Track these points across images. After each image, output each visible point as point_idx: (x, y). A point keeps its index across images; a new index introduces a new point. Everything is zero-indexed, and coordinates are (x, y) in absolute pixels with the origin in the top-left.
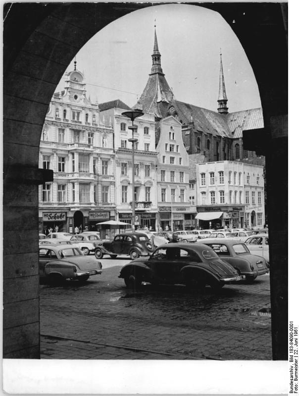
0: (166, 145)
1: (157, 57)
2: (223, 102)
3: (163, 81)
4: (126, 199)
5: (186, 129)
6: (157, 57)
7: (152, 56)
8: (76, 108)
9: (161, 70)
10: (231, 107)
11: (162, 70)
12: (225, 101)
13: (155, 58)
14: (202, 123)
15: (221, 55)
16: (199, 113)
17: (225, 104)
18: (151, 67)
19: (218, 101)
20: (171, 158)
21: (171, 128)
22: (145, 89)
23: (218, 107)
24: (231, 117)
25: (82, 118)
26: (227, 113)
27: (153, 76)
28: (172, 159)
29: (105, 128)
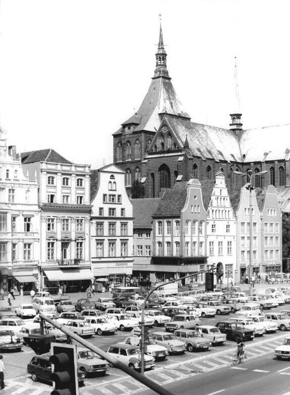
0: (105, 195)
1: (162, 57)
3: (169, 87)
5: (179, 154)
6: (162, 57)
7: (156, 55)
9: (167, 73)
11: (167, 73)
13: (160, 58)
14: (202, 145)
16: (201, 132)
17: (239, 118)
19: (231, 115)
20: (110, 209)
21: (112, 177)
24: (244, 136)
28: (112, 210)
29: (28, 183)
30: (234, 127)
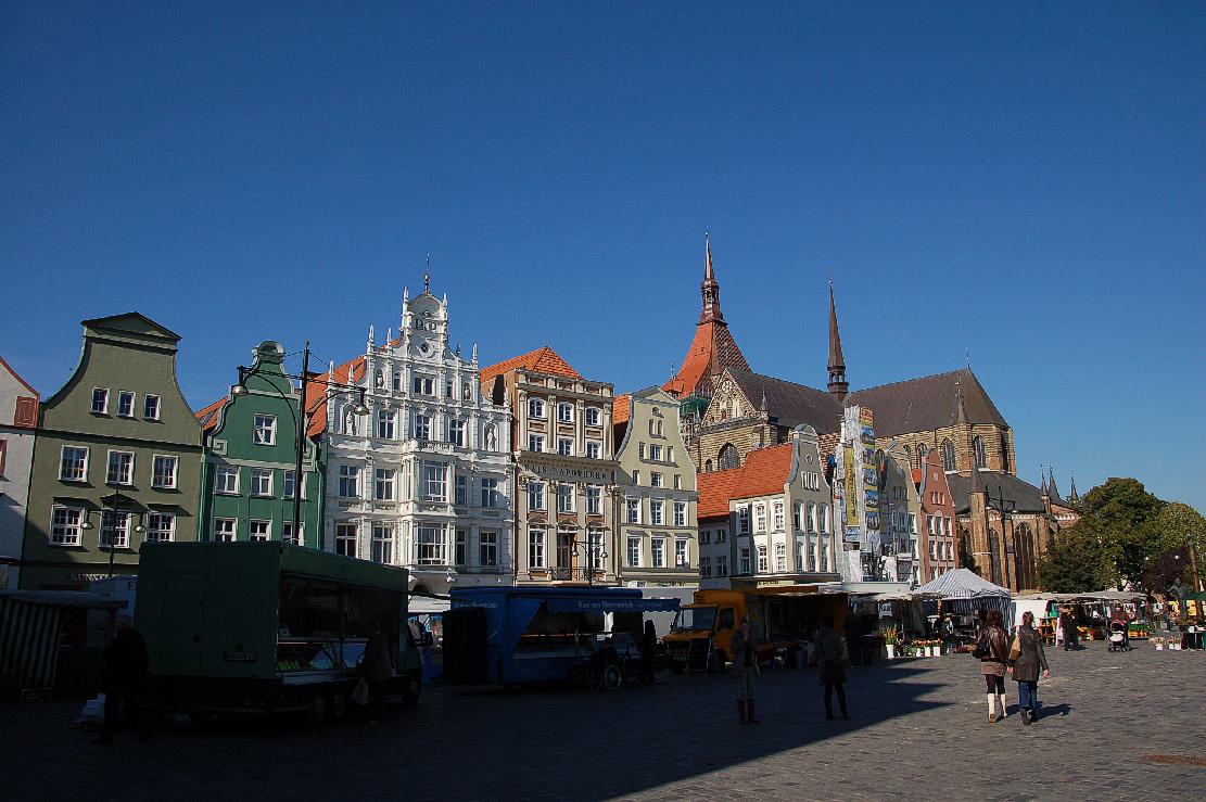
0: (642, 446)
4: (540, 560)
8: (423, 370)
12: (841, 369)
21: (654, 410)
25: (438, 389)
28: (655, 477)
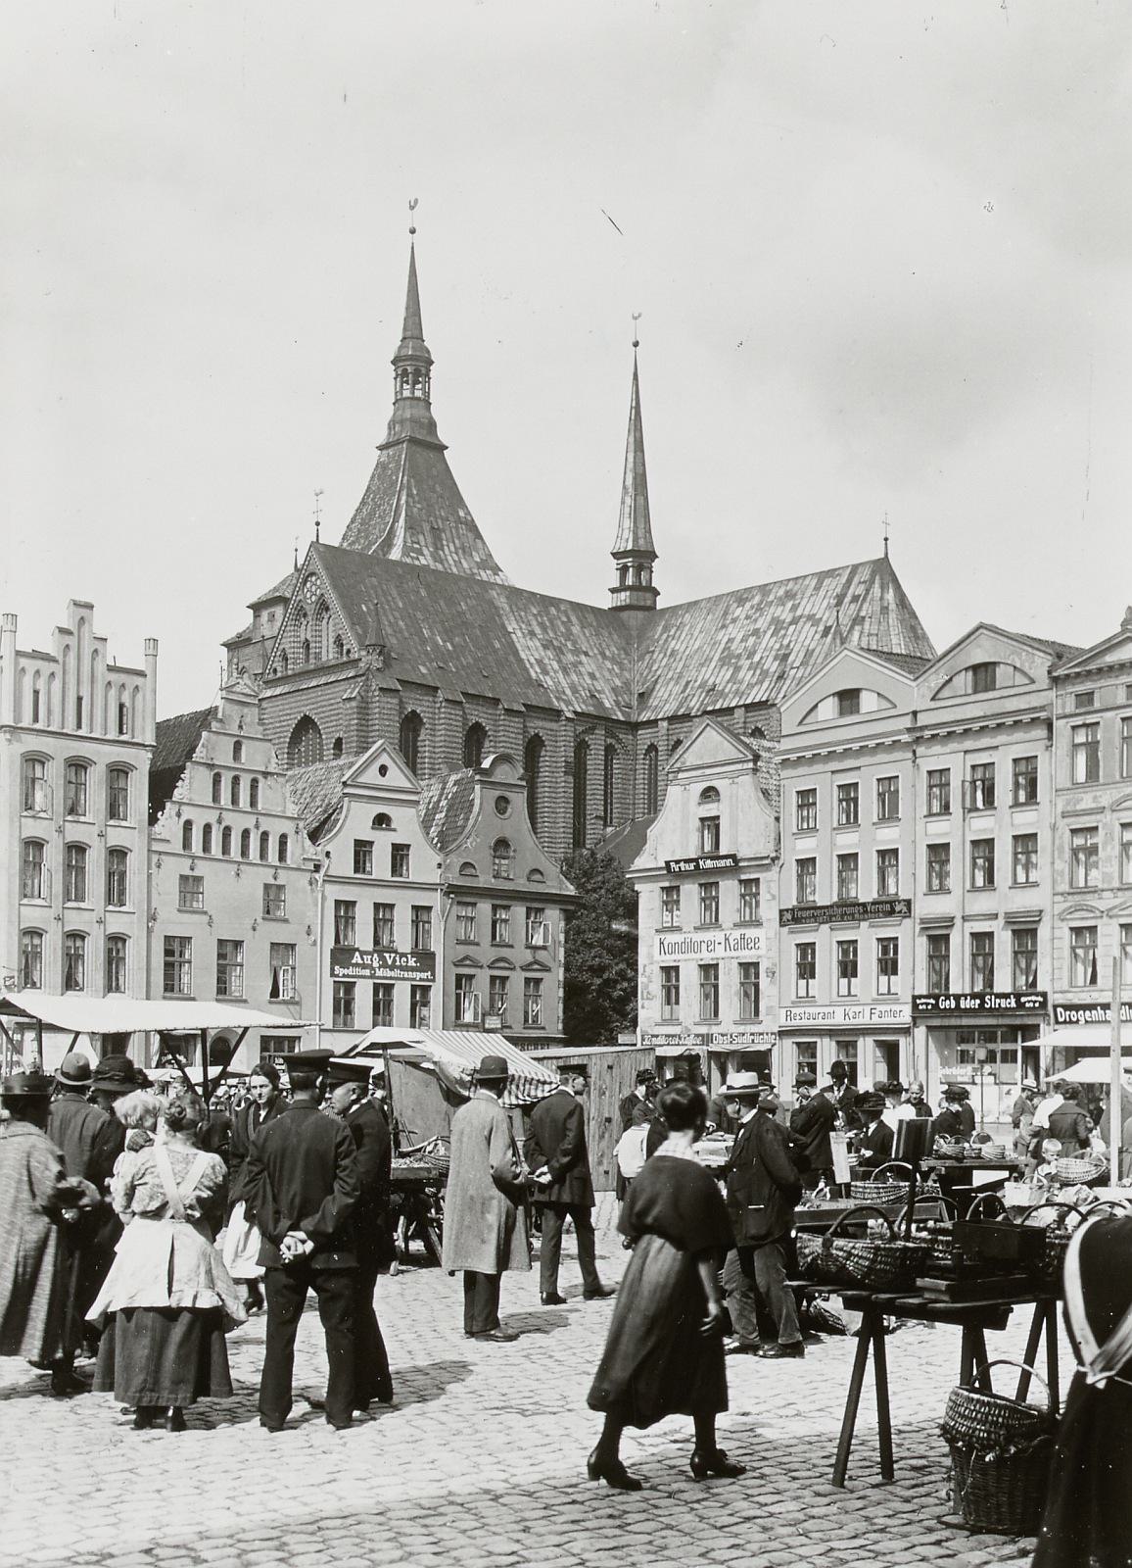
1: (414, 365)
2: (638, 559)
6: (414, 365)
7: (393, 362)
9: (432, 426)
10: (670, 586)
13: (405, 373)
15: (636, 344)
18: (388, 411)
22: (359, 510)
23: (616, 584)
26: (653, 608)
27: (391, 452)
30: (624, 597)
